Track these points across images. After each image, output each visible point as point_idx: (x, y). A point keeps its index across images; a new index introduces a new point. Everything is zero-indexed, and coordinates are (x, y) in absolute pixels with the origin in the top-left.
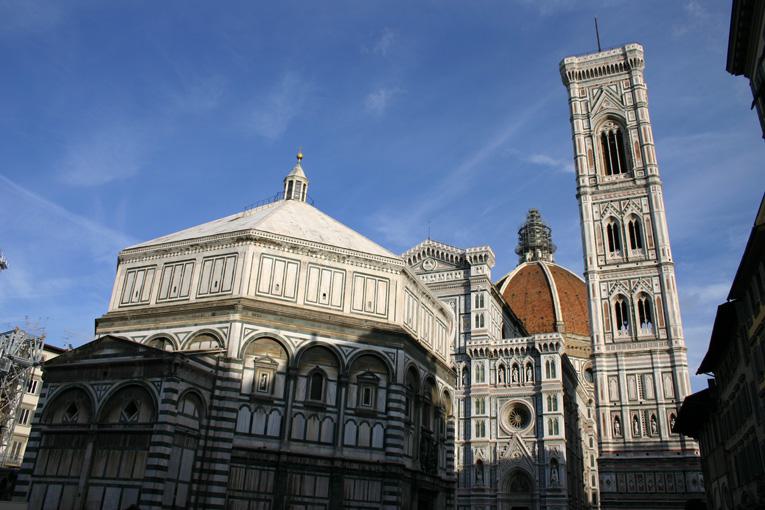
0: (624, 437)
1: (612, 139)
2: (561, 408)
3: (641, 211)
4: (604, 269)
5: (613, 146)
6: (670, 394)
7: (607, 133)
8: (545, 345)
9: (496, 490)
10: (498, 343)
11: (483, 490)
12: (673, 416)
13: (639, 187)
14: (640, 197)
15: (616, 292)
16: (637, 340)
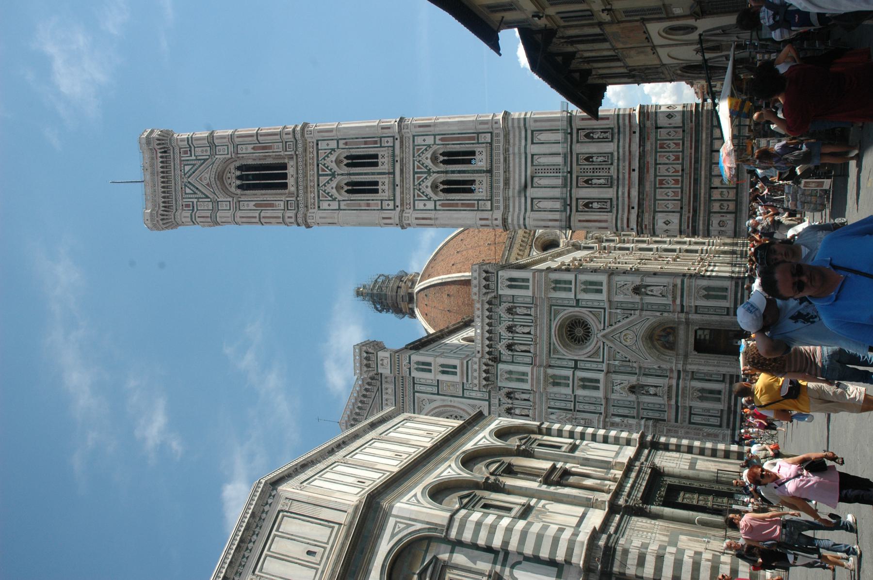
0: (611, 199)
1: (246, 177)
2: (570, 277)
3: (333, 150)
4: (398, 203)
5: (256, 177)
6: (559, 136)
7: (239, 182)
8: (487, 287)
9: (671, 370)
10: (479, 349)
11: (670, 387)
12: (587, 136)
13: (305, 150)
14: (318, 150)
15: (429, 191)
16: (490, 171)
